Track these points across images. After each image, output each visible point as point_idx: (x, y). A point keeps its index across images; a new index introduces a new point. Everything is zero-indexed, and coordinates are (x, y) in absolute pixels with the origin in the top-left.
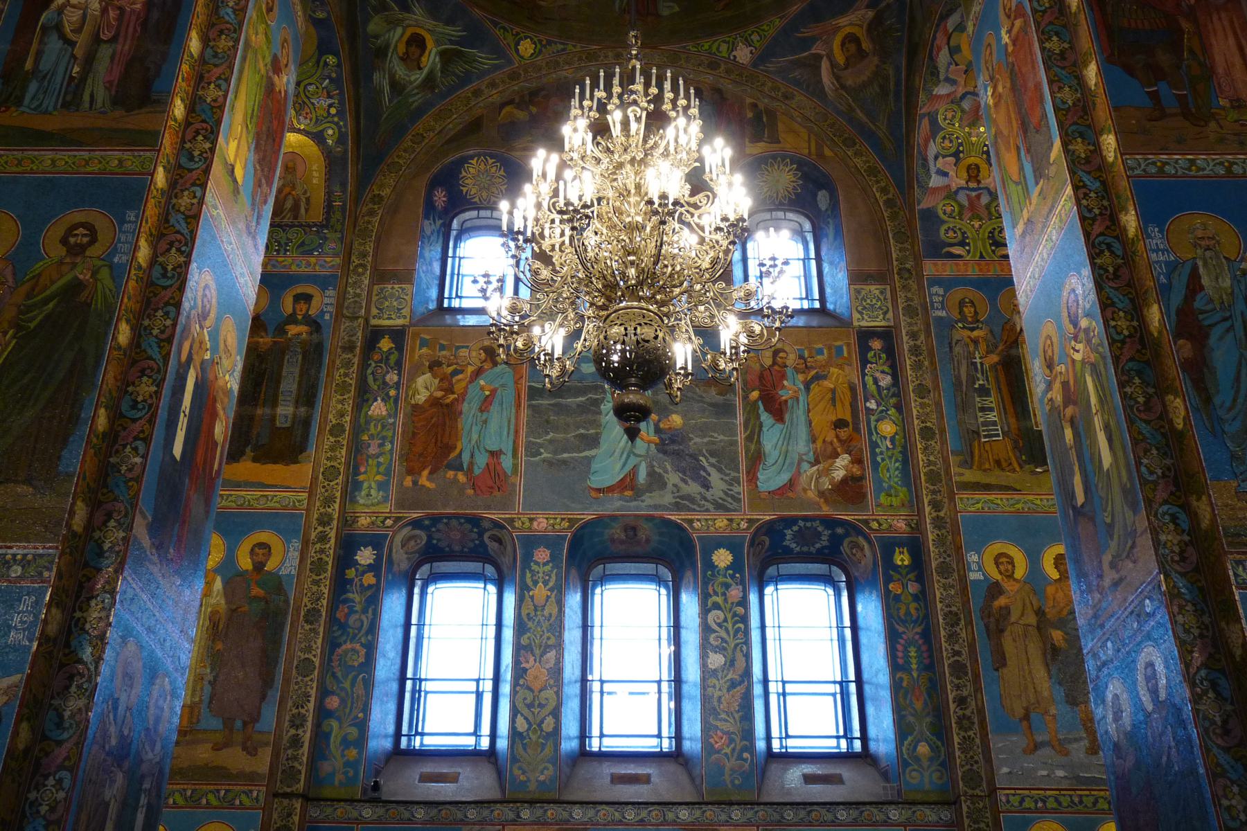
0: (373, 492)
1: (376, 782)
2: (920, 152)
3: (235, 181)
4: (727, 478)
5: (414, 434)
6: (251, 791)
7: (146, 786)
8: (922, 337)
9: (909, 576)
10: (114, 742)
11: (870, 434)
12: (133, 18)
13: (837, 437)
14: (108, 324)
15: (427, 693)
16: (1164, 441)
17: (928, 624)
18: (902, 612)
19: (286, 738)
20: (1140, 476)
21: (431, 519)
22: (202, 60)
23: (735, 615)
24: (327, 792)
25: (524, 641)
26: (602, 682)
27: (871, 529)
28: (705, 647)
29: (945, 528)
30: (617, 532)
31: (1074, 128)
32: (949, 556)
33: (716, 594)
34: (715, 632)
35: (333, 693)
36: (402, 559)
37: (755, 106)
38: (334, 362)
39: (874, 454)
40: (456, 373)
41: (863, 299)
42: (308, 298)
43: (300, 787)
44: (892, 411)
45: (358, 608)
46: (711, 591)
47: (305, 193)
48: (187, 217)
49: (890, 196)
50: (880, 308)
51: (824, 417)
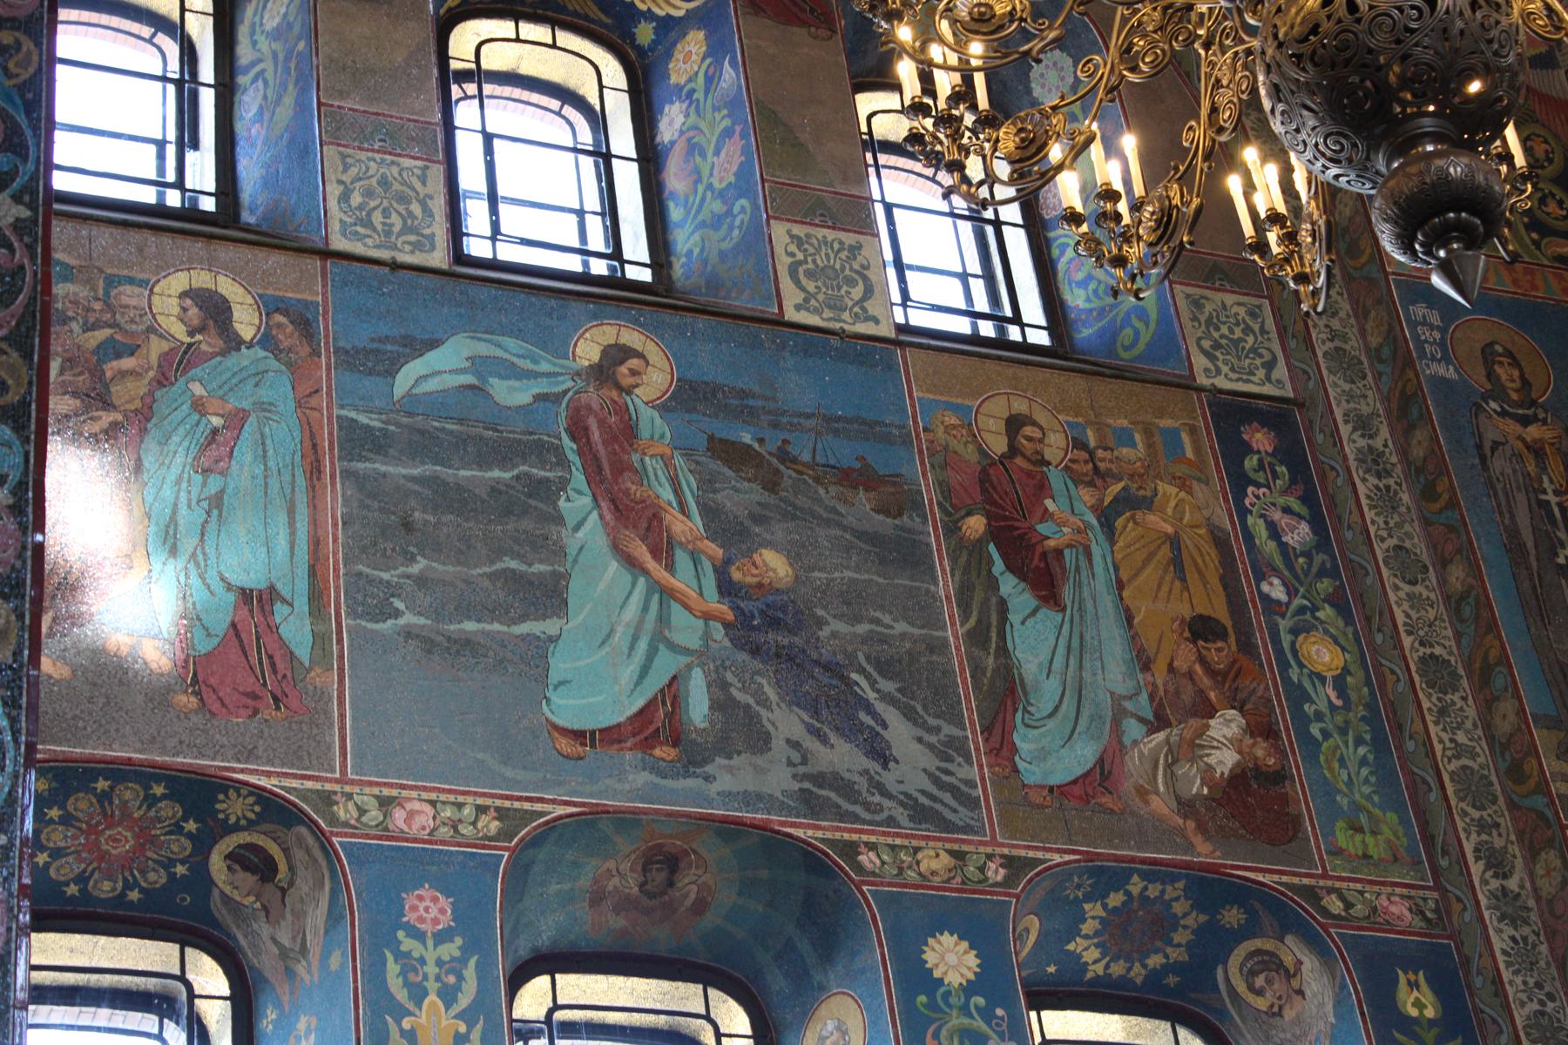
4: (933, 739)
13: (1202, 660)
29: (1526, 922)
32: (1551, 997)
44: (1326, 613)
50: (1253, 350)
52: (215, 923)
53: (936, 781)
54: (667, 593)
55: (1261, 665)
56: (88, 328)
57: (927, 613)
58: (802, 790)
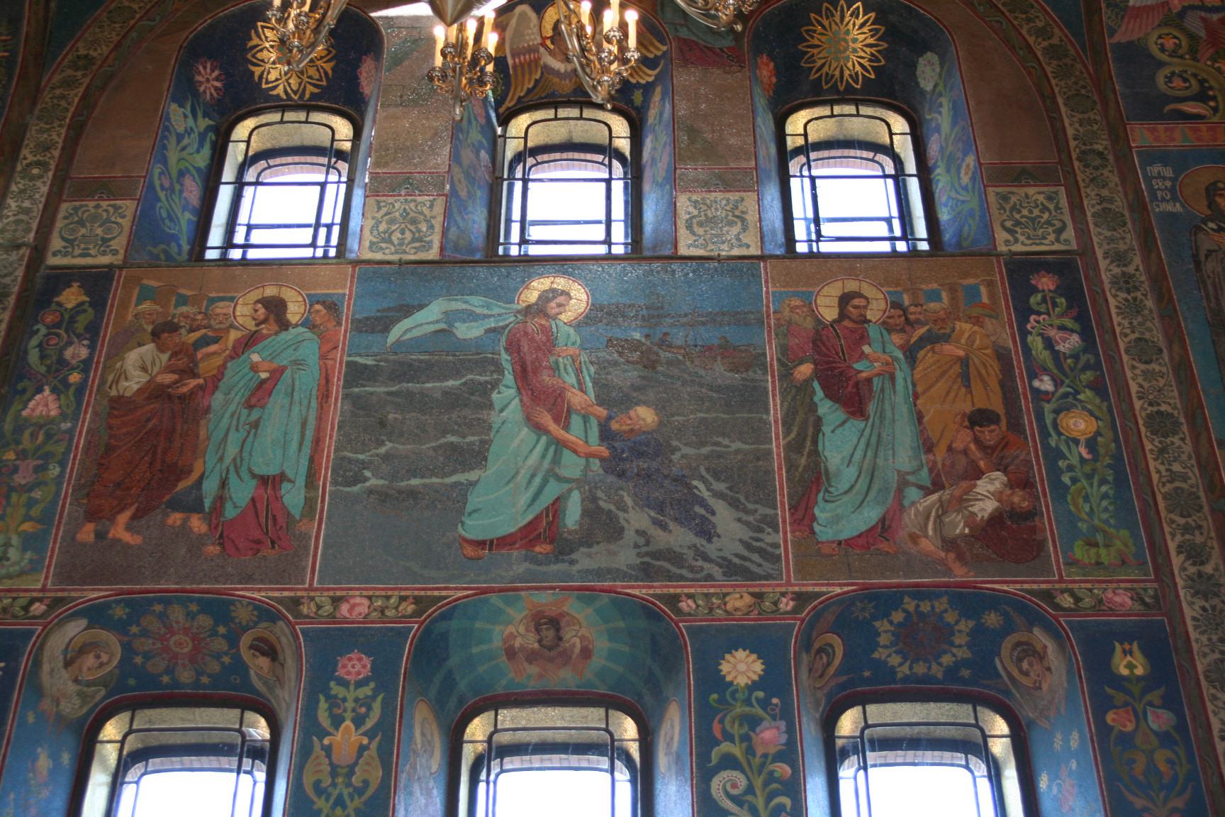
4: (751, 519)
5: (110, 449)
9: (1148, 697)
11: (1045, 434)
13: (977, 441)
18: (1140, 766)
21: (128, 603)
23: (771, 778)
27: (1057, 607)
29: (1216, 595)
33: (729, 738)
39: (1054, 473)
40: (205, 341)
41: (1013, 208)
44: (1086, 395)
50: (1049, 223)
52: (259, 694)
53: (747, 546)
54: (560, 444)
55: (1026, 438)
56: (192, 330)
57: (759, 433)
58: (642, 563)
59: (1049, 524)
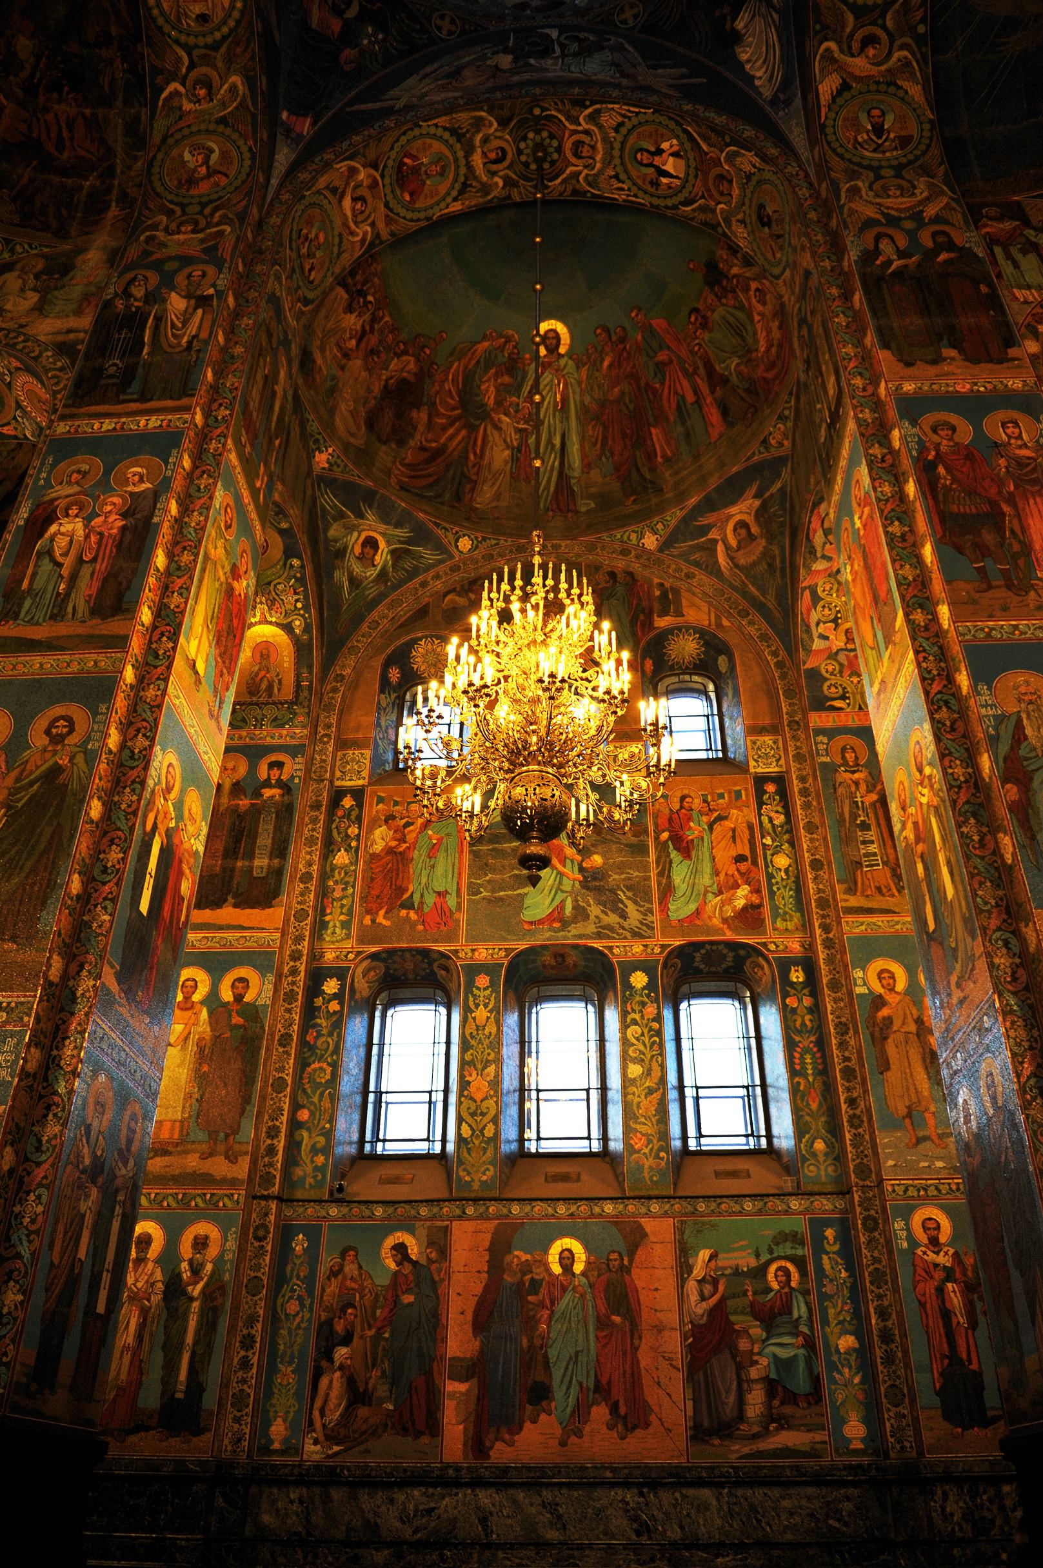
0: (337, 930)
1: (340, 1185)
2: (803, 620)
3: (197, 673)
5: (372, 880)
6: (232, 1195)
7: (121, 1197)
8: (810, 780)
10: (87, 1161)
11: (767, 867)
12: (111, 541)
13: (738, 870)
14: (82, 802)
15: (387, 1103)
16: (997, 874)
17: (821, 1033)
18: (798, 1024)
19: (263, 1148)
20: (976, 907)
22: (168, 572)
23: (651, 1030)
24: (299, 1195)
25: (468, 1057)
26: (538, 1091)
27: (769, 950)
28: (625, 1059)
30: (548, 959)
31: (914, 600)
33: (634, 1011)
34: (633, 1045)
35: (303, 1107)
36: (363, 987)
37: (662, 585)
38: (303, 819)
39: (770, 885)
40: (407, 825)
41: (758, 749)
42: (280, 765)
43: (275, 1190)
44: (786, 846)
45: (325, 1032)
46: (629, 1009)
47: (278, 675)
48: (152, 707)
49: (780, 658)
51: (725, 854)
53: (641, 923)
57: (646, 869)
59: (767, 912)
